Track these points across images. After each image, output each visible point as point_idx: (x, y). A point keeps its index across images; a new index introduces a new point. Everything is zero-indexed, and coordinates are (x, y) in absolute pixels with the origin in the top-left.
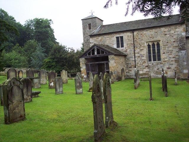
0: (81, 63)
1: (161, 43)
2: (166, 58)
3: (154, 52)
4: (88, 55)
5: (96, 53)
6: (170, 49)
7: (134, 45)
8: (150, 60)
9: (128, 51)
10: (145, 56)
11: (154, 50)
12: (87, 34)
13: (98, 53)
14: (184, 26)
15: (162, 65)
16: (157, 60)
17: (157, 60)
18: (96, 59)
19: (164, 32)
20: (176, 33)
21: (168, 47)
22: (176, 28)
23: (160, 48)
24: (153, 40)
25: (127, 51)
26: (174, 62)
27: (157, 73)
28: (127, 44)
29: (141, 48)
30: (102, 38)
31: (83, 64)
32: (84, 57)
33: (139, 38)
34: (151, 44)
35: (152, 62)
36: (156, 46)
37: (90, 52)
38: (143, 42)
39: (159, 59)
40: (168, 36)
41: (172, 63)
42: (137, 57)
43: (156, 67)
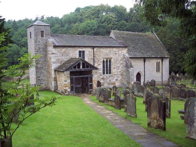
1: (112, 60)
3: (107, 67)
4: (73, 69)
5: (81, 67)
6: (118, 65)
7: (94, 59)
8: (104, 73)
11: (107, 65)
12: (39, 42)
13: (83, 67)
14: (127, 49)
15: (112, 77)
16: (108, 73)
17: (108, 73)
18: (81, 73)
19: (115, 51)
22: (123, 50)
24: (107, 57)
26: (120, 76)
27: (109, 84)
28: (89, 58)
29: (99, 63)
32: (69, 70)
35: (106, 74)
39: (110, 73)
40: (117, 55)
41: (119, 76)
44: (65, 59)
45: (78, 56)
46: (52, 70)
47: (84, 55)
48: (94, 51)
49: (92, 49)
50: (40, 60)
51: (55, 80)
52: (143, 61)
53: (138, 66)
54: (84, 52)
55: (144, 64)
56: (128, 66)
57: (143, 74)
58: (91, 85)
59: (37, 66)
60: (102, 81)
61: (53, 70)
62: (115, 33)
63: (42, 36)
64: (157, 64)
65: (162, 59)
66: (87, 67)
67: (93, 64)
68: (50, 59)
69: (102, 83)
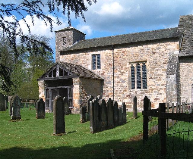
0: (40, 88)
2: (154, 85)
3: (139, 77)
5: (58, 74)
6: (159, 73)
7: (113, 66)
9: (106, 74)
10: (127, 81)
11: (139, 74)
13: (61, 74)
16: (142, 87)
17: (142, 87)
18: (57, 82)
20: (168, 52)
23: (147, 71)
24: (138, 60)
25: (104, 74)
26: (163, 92)
29: (122, 71)
30: (74, 56)
31: (42, 88)
33: (120, 57)
34: (135, 65)
35: (136, 89)
36: (141, 69)
37: (51, 73)
38: (124, 62)
39: (145, 87)
40: (157, 55)
41: (160, 92)
42: (117, 83)
54: (100, 54)
58: (71, 100)
69: (127, 103)
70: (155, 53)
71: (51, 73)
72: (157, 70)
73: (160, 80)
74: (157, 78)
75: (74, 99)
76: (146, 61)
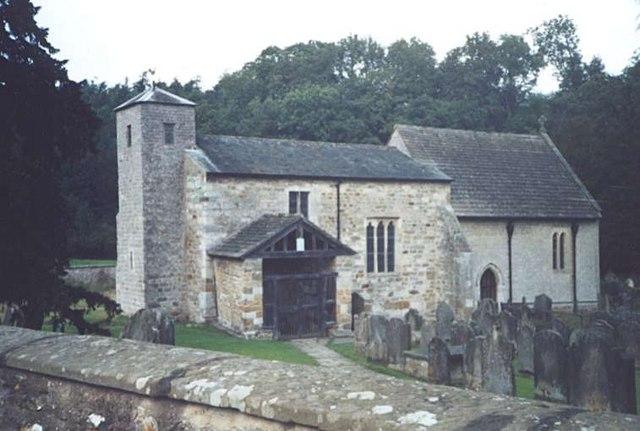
1: (399, 225)
2: (410, 266)
3: (381, 248)
6: (419, 242)
7: (338, 222)
8: (370, 269)
11: (381, 242)
12: (159, 159)
15: (400, 284)
16: (386, 268)
17: (386, 268)
19: (410, 196)
20: (433, 204)
21: (415, 238)
22: (433, 192)
24: (382, 214)
27: (388, 305)
29: (355, 234)
30: (246, 188)
32: (260, 255)
33: (351, 206)
34: (375, 224)
36: (386, 232)
38: (359, 216)
39: (391, 268)
40: (416, 208)
41: (420, 278)
43: (388, 289)
44: (246, 218)
45: (286, 210)
46: (199, 252)
47: (304, 206)
48: (338, 194)
49: (331, 186)
50: (160, 219)
51: (211, 286)
52: (505, 231)
53: (487, 247)
54: (305, 195)
55: (509, 242)
56: (453, 246)
57: (506, 275)
58: (332, 308)
59: (150, 240)
60: (365, 295)
61: (204, 253)
62: (403, 134)
63: (169, 140)
64: (555, 241)
65: (575, 224)
66: (320, 245)
67: (335, 236)
68: (194, 217)
70: (412, 204)
71: (282, 240)
72: (415, 238)
73: (420, 256)
74: (414, 252)
75: (338, 301)
76: (398, 218)
